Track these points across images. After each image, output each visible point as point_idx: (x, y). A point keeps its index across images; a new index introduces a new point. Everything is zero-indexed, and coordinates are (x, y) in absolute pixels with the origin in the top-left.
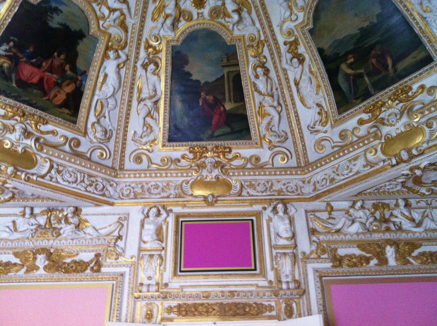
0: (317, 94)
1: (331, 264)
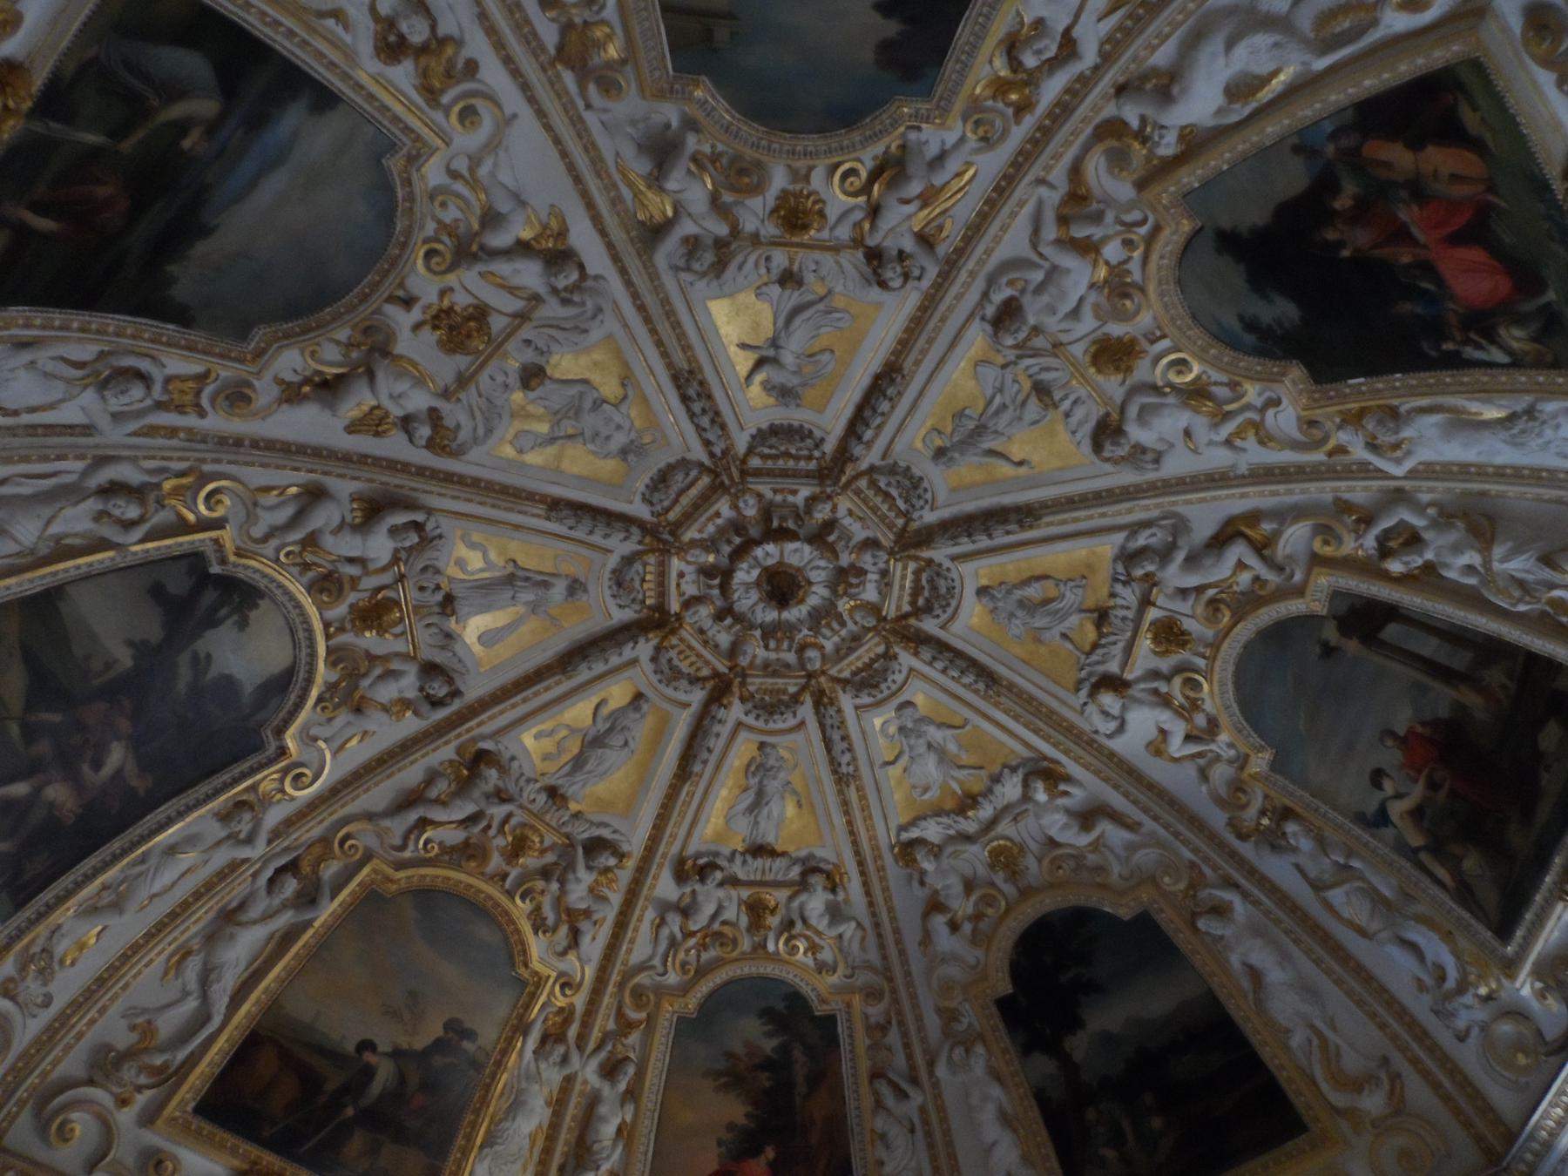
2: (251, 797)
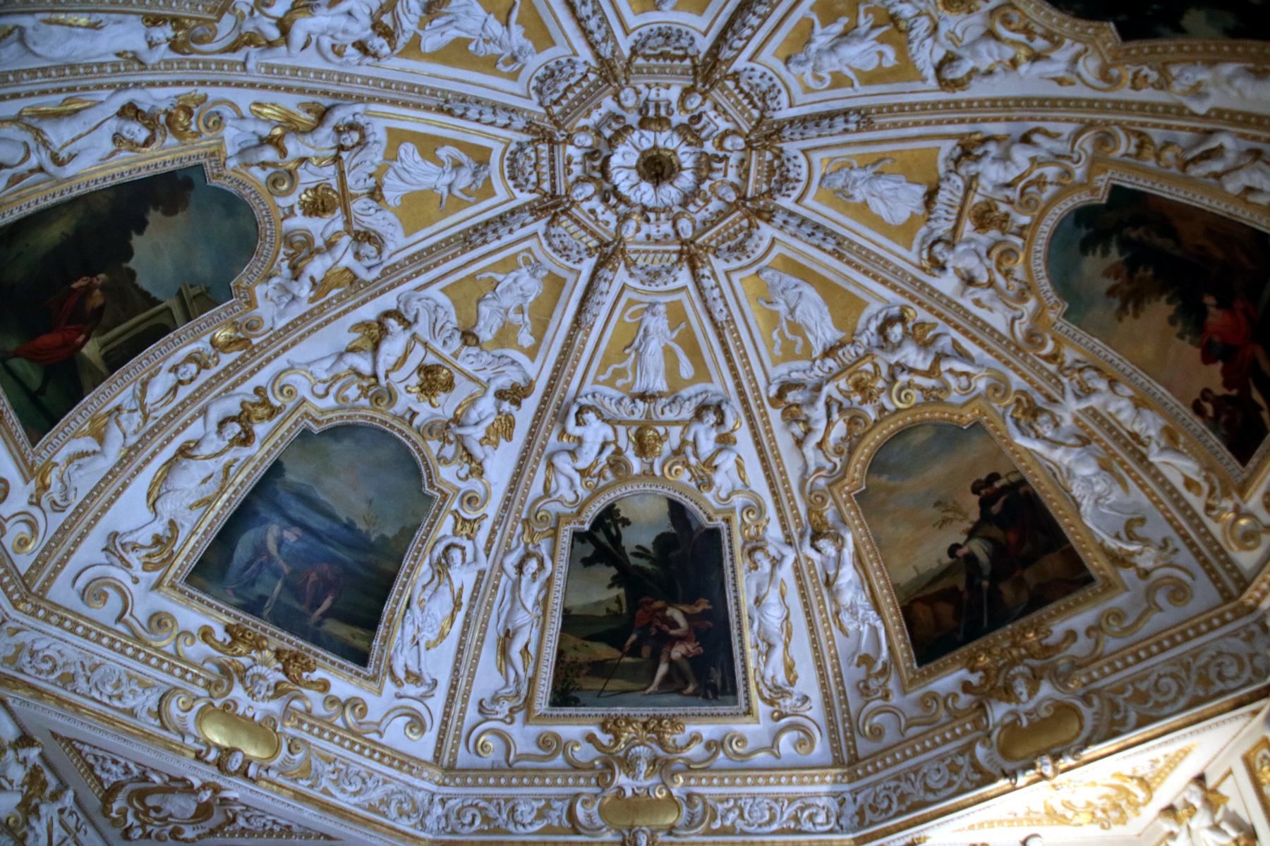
0: (191, 508)
2: (748, 546)
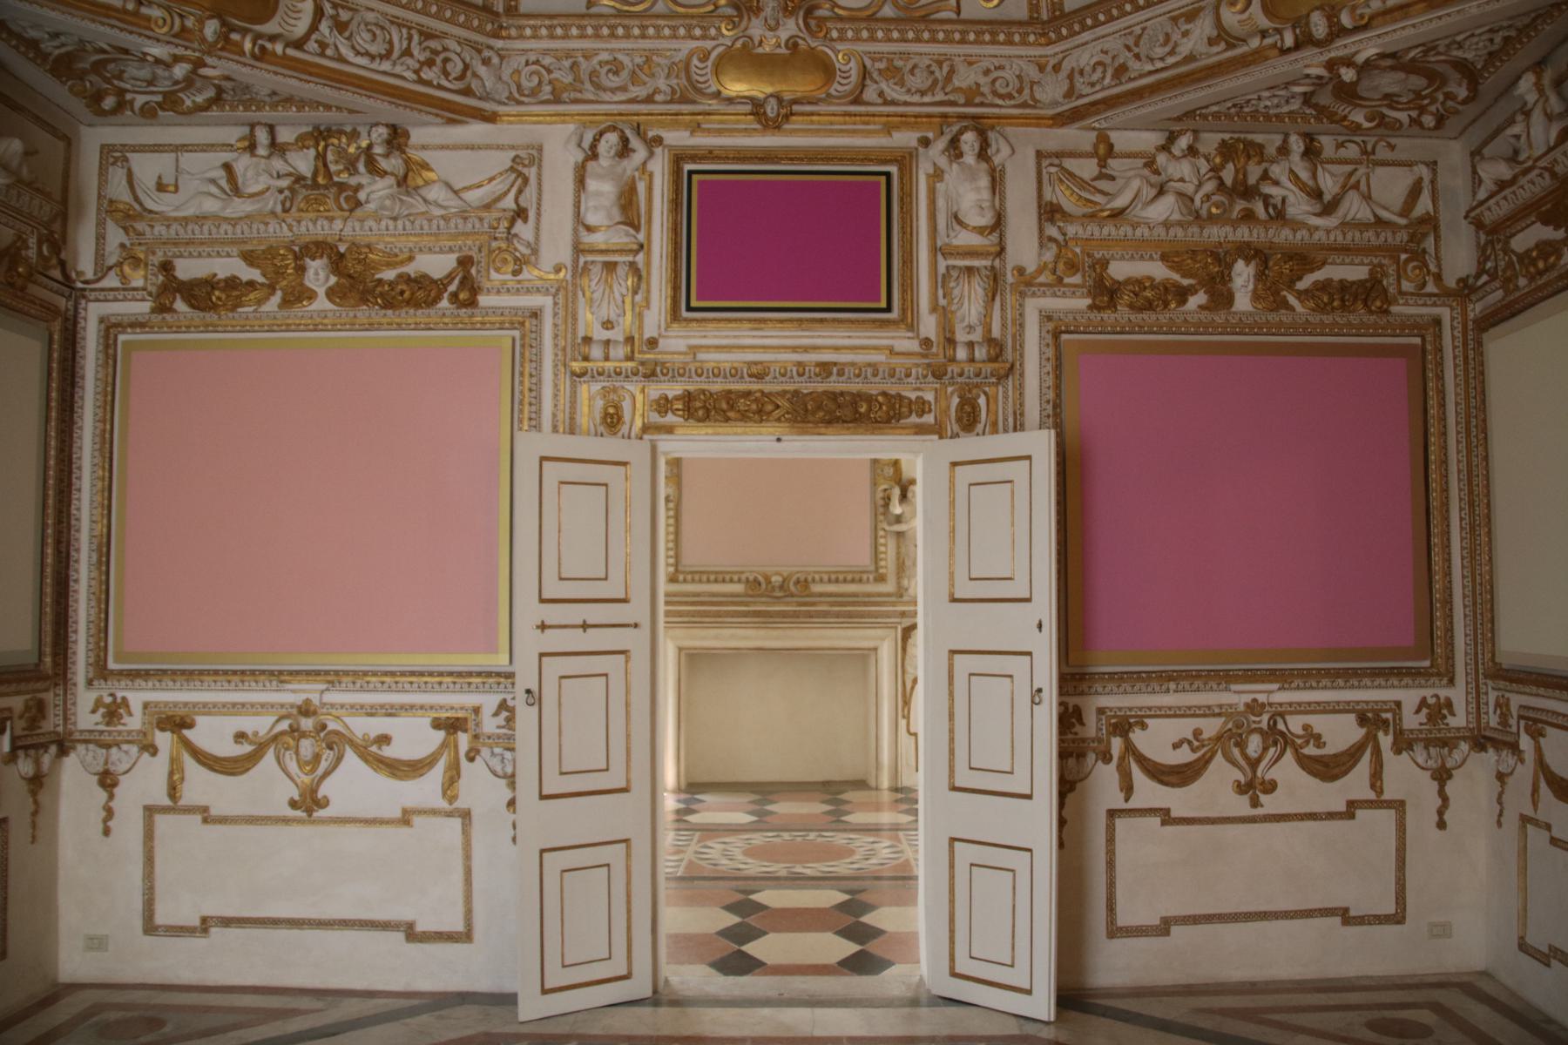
1: (1088, 301)
